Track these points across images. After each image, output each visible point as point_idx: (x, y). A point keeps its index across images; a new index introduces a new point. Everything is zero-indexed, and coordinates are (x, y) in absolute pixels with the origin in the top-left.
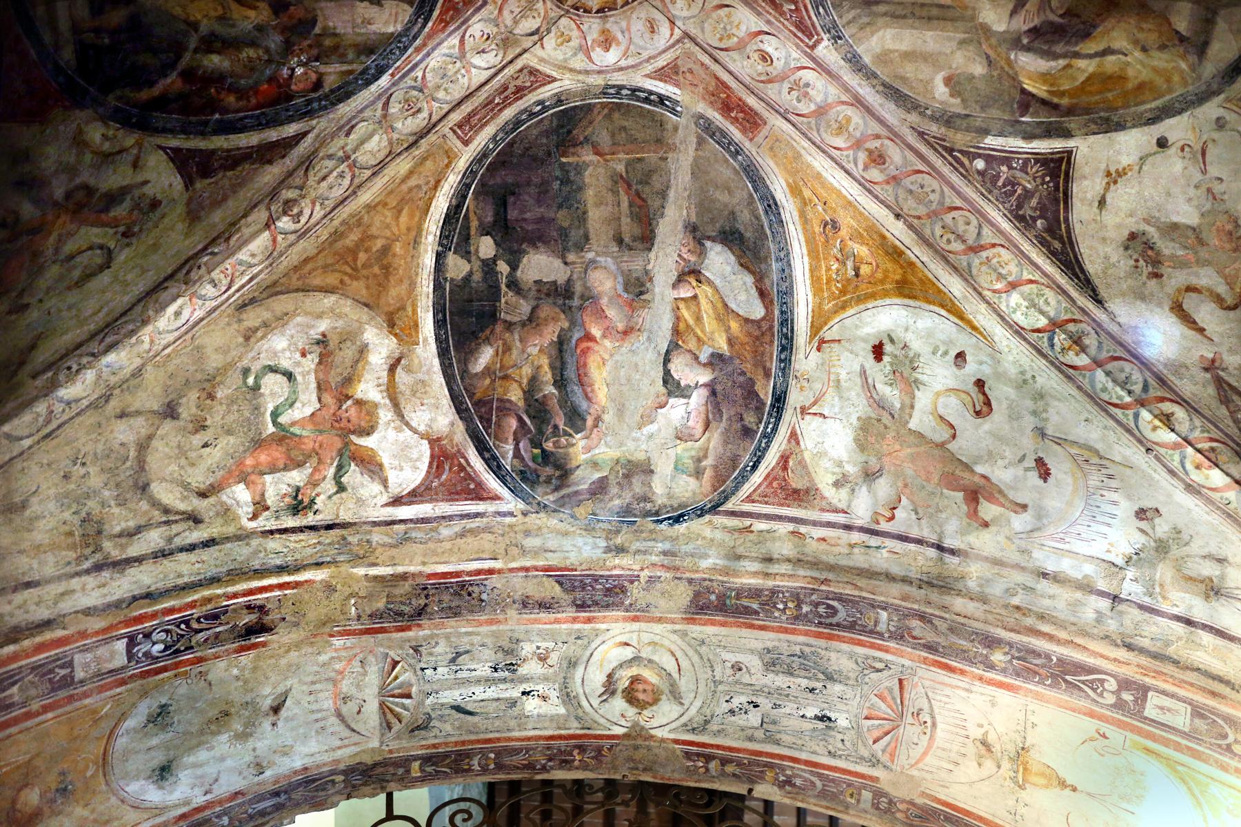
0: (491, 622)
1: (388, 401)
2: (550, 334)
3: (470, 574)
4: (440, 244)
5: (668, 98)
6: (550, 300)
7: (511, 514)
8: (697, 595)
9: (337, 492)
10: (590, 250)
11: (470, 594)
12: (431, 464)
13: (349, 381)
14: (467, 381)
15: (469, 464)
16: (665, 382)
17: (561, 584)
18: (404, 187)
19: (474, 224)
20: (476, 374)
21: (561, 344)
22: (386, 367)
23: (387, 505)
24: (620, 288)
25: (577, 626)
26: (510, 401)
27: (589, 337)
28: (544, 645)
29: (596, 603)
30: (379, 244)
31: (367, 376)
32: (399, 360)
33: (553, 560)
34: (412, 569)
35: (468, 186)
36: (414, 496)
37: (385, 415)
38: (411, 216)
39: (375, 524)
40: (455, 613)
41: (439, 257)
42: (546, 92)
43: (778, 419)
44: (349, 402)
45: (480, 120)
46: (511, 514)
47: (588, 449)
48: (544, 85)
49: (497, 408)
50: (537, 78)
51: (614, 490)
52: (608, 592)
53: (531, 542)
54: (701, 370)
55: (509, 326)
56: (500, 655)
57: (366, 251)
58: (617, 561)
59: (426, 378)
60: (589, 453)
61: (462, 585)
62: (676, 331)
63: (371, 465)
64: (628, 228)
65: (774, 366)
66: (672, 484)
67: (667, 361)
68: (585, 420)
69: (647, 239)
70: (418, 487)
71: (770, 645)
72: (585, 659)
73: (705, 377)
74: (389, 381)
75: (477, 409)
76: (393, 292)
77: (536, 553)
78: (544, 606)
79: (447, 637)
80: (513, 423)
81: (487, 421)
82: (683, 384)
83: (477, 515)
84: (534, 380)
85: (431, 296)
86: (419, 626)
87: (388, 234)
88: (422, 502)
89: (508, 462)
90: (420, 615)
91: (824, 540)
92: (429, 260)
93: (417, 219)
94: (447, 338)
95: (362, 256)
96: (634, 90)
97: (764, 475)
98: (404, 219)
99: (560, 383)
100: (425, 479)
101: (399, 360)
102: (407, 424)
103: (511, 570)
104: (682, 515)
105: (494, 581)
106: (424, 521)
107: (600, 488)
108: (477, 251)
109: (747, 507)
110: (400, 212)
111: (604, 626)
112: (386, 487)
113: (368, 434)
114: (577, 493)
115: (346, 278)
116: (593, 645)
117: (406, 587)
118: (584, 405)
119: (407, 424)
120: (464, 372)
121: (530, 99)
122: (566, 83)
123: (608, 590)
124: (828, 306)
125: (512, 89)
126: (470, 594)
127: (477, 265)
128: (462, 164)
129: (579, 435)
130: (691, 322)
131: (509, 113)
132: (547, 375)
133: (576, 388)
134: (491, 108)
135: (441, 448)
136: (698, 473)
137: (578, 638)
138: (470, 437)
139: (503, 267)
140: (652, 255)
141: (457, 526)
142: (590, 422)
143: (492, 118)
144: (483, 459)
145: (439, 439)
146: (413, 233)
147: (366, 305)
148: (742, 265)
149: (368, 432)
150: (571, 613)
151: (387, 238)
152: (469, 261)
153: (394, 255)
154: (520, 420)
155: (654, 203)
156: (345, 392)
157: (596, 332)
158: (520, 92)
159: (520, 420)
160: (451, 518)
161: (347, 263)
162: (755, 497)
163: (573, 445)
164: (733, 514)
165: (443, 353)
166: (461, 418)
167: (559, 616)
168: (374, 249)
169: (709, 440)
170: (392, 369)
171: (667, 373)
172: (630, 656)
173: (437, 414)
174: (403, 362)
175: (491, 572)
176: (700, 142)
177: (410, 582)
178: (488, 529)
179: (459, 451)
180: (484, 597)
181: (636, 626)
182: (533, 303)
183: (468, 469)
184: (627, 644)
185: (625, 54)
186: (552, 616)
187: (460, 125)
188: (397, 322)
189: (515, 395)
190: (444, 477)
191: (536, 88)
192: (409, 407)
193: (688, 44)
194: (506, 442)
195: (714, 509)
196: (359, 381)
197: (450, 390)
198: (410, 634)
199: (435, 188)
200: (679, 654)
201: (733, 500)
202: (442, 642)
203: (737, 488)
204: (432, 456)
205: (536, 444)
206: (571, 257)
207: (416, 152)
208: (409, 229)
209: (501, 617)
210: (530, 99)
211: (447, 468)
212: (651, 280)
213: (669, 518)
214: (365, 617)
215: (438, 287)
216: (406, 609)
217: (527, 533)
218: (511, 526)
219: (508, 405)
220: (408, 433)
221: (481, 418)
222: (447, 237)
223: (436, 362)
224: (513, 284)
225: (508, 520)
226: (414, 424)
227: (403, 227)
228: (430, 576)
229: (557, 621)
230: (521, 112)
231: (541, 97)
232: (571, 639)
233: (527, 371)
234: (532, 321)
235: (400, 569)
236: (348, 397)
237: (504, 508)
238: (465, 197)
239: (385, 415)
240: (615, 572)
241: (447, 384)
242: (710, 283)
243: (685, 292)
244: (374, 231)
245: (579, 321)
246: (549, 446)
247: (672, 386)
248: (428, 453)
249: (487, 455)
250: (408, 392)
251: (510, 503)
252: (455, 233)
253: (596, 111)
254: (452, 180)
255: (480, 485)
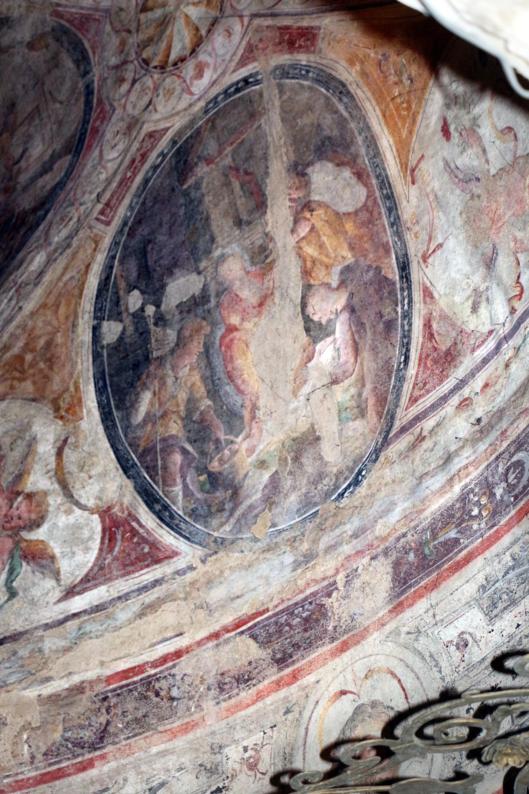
0: (186, 729)
1: (56, 486)
2: (196, 346)
3: (154, 664)
4: (95, 318)
5: (251, 76)
6: (191, 316)
7: (191, 568)
8: (397, 565)
9: (9, 600)
10: (217, 248)
11: (157, 694)
12: (103, 538)
13: (20, 477)
14: (131, 435)
15: (141, 526)
16: (307, 330)
17: (254, 637)
18: (61, 284)
19: (122, 285)
20: (139, 425)
21: (207, 353)
22: (53, 451)
23: (59, 601)
24: (247, 264)
25: (283, 693)
26: (172, 437)
27: (232, 329)
28: (249, 742)
29: (296, 646)
30: (42, 342)
31: (36, 467)
32: (65, 441)
33: (244, 609)
34: (91, 675)
35: (113, 257)
36: (88, 581)
37: (55, 500)
38: (68, 305)
39: (47, 626)
40: (140, 725)
41: (96, 329)
42: (163, 143)
43: (409, 288)
44: (20, 499)
45: (118, 199)
46: (191, 568)
47: (251, 451)
48: (162, 137)
49: (161, 450)
50: (153, 136)
51: (287, 483)
52: (308, 623)
53: (217, 594)
54: (334, 296)
55: (161, 359)
56: (203, 778)
57: (33, 351)
58: (309, 575)
59: (92, 449)
60: (253, 453)
61: (148, 682)
62: (306, 273)
63: (39, 557)
64: (242, 203)
65: (389, 237)
66: (340, 443)
67: (304, 305)
68: (242, 418)
69: (261, 205)
70: (91, 570)
71: (481, 578)
72: (301, 742)
73: (340, 301)
74: (58, 465)
75: (140, 462)
76: (57, 379)
77: (223, 606)
78: (244, 679)
79: (136, 767)
80: (177, 458)
81: (151, 469)
82: (324, 322)
83: (156, 583)
84: (191, 402)
85: (91, 368)
86: (103, 757)
87: (50, 328)
88: (96, 586)
89: (178, 508)
90: (102, 739)
91: (486, 385)
92: (85, 335)
93: (73, 306)
94: (109, 401)
95: (29, 357)
96: (225, 92)
97: (417, 361)
98: (62, 310)
99: (214, 392)
100: (97, 559)
101: (65, 441)
102: (78, 504)
103: (199, 644)
104: (359, 473)
105: (185, 666)
106: (98, 608)
107: (274, 491)
108: (127, 309)
109: (414, 411)
110: (58, 306)
111: (310, 679)
112: (58, 580)
113: (39, 526)
114: (251, 507)
115: (15, 383)
116: (306, 714)
117: (84, 702)
118: (238, 400)
119: (78, 504)
120: (127, 428)
121: (153, 158)
122: (178, 123)
123: (306, 620)
124: (404, 134)
125: (139, 158)
126: (157, 694)
127: (128, 321)
128: (107, 241)
129: (240, 438)
130: (316, 254)
131: (139, 179)
132: (201, 390)
133: (227, 388)
134: (124, 183)
135: (111, 517)
136: (362, 413)
137: (288, 711)
138: (139, 493)
139: (150, 310)
140: (269, 216)
141: (134, 605)
142: (246, 414)
143: (127, 191)
144: (154, 512)
145: (109, 508)
146: (71, 319)
147: (34, 400)
148: (338, 165)
149: (36, 524)
150: (273, 675)
151: (49, 334)
152: (121, 321)
153: (57, 345)
154: (184, 452)
155: (259, 171)
156: (16, 489)
157: (235, 320)
158: (144, 157)
159: (184, 452)
160: (124, 598)
161: (16, 369)
162: (417, 393)
163: (237, 451)
164: (403, 430)
165: (106, 417)
166: (128, 477)
167: (261, 686)
168: (38, 348)
169: (362, 364)
170: (59, 453)
171: (307, 319)
172: (350, 711)
173: (105, 482)
174: (69, 441)
175: (178, 654)
176: (281, 89)
177: (88, 693)
178: (170, 597)
179: (130, 514)
180: (175, 693)
181: (346, 657)
182: (177, 327)
183: (141, 531)
184: (343, 693)
185: (215, 70)
186: (253, 691)
187: (102, 213)
188: (65, 409)
189: (175, 428)
190: (117, 549)
191: (156, 145)
192: (78, 485)
193: (257, 22)
194: (175, 485)
195: (386, 442)
196: (29, 474)
197: (116, 451)
198: (93, 772)
199: (87, 272)
200: (399, 671)
201: (399, 413)
202: (132, 776)
203: (398, 397)
204: (104, 531)
205: (202, 470)
206: (203, 265)
207: (69, 251)
208: (67, 318)
209: (196, 717)
210: (153, 158)
211: (119, 537)
212: (272, 239)
213: (349, 486)
214: (39, 757)
215: (96, 356)
216: (87, 735)
217: (210, 583)
218: (193, 584)
219: (171, 442)
220: (78, 512)
221: (147, 468)
222: (100, 309)
223: (100, 429)
224: (161, 320)
225: (190, 576)
226: (83, 501)
227: (62, 318)
228: (109, 680)
229: (260, 697)
230: (147, 172)
231: (160, 150)
232: (279, 718)
233: (182, 396)
234: (181, 343)
235: (76, 679)
236: (18, 494)
237: (180, 563)
238: (111, 267)
239: (55, 500)
240: (308, 592)
241: (112, 446)
242: (320, 204)
243: (304, 230)
244: (38, 332)
245: (219, 318)
246: (215, 466)
247: (315, 331)
248: (99, 528)
249: (158, 507)
250: (76, 470)
251: (187, 552)
252: (108, 303)
253: (202, 130)
254: (101, 258)
255: (154, 545)
